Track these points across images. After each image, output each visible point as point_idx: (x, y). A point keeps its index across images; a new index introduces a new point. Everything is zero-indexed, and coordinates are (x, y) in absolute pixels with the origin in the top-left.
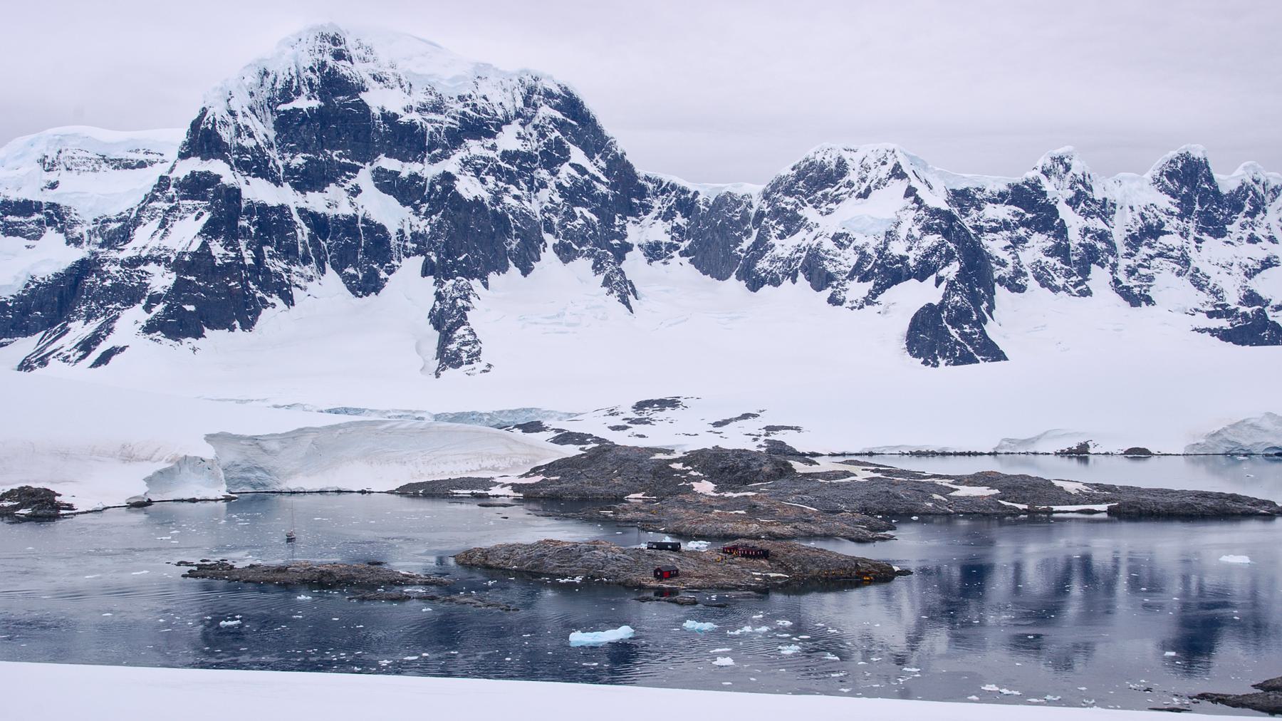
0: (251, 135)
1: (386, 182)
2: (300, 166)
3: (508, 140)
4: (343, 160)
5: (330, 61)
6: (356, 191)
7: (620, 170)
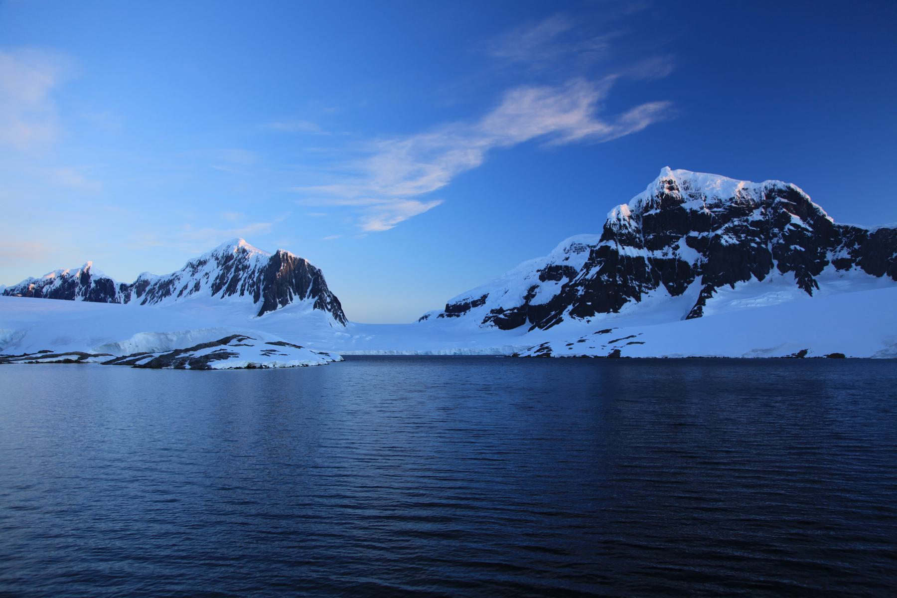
0: (626, 228)
1: (691, 242)
2: (651, 239)
4: (672, 234)
5: (666, 191)
6: (677, 247)
7: (820, 222)
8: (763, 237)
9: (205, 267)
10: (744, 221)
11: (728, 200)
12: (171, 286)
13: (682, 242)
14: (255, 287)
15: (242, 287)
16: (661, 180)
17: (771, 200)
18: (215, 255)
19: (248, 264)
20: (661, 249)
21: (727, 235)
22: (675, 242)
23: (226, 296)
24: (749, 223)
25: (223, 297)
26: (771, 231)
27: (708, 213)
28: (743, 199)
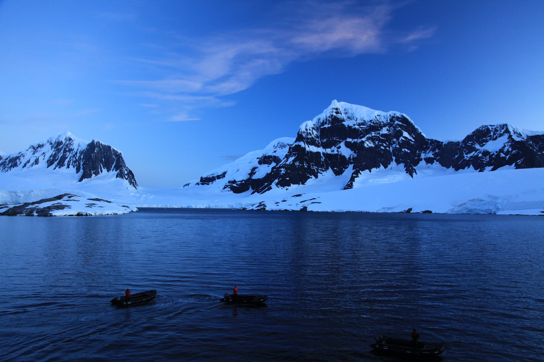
0: (311, 135)
1: (348, 145)
3: (384, 131)
4: (337, 140)
5: (334, 114)
6: (340, 147)
7: (419, 137)
8: (387, 143)
9: (42, 149)
10: (378, 134)
11: (369, 121)
12: (18, 161)
13: (342, 144)
14: (77, 163)
15: (68, 162)
16: (332, 107)
17: (393, 123)
18: (50, 141)
19: (73, 148)
20: (331, 148)
21: (368, 141)
22: (338, 144)
23: (57, 168)
24: (380, 135)
25: (55, 168)
26: (392, 140)
27: (357, 128)
28: (377, 121)
